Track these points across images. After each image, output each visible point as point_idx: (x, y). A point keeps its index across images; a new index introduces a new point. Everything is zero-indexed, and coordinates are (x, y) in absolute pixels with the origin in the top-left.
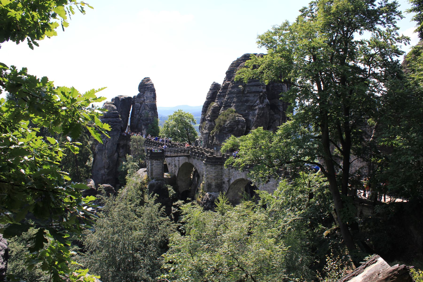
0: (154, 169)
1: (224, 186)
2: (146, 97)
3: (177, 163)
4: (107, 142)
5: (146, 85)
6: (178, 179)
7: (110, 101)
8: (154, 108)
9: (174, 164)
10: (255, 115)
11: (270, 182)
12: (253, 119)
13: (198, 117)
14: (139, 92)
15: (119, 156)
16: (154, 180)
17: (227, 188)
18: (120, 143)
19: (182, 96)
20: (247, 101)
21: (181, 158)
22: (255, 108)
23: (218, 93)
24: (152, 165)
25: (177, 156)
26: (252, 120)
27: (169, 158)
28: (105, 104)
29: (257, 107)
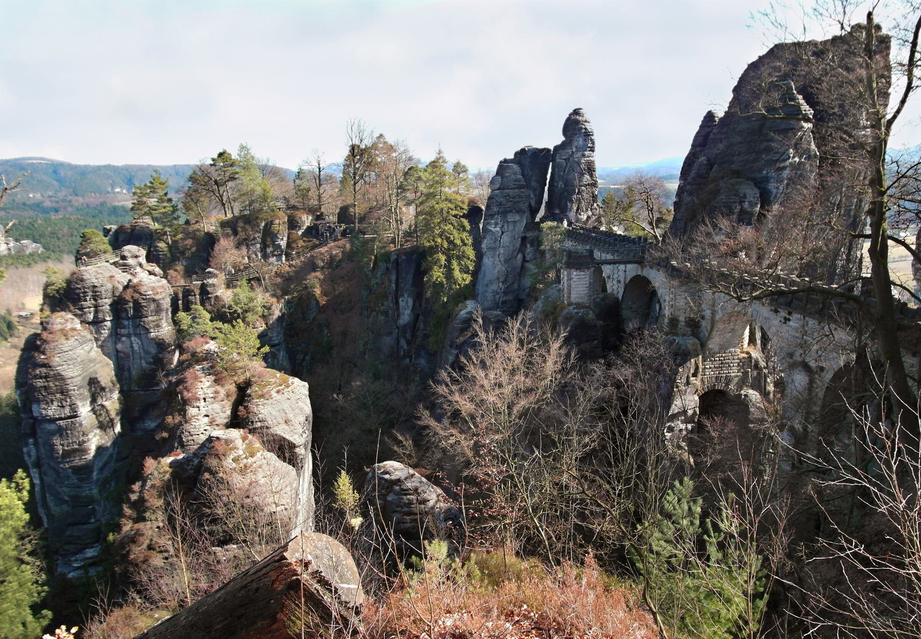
0: (573, 286)
1: (704, 323)
2: (576, 147)
3: (621, 274)
4: (503, 233)
5: (577, 122)
6: (623, 306)
7: (512, 157)
8: (591, 169)
9: (617, 277)
10: (782, 181)
11: (791, 323)
12: (778, 188)
13: (674, 186)
14: (564, 139)
15: (524, 260)
16: (571, 308)
17: (709, 328)
18: (528, 235)
19: (644, 144)
20: (769, 150)
21: (629, 266)
22: (782, 165)
23: (712, 136)
24: (570, 279)
25: (620, 262)
26: (775, 191)
27: (608, 266)
28: (501, 162)
29: (787, 163)
